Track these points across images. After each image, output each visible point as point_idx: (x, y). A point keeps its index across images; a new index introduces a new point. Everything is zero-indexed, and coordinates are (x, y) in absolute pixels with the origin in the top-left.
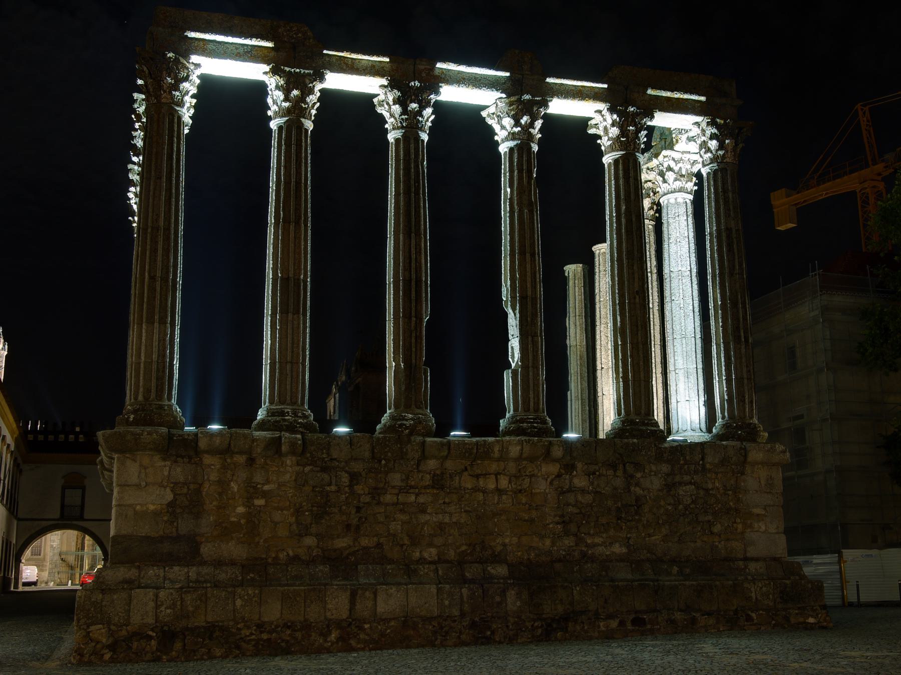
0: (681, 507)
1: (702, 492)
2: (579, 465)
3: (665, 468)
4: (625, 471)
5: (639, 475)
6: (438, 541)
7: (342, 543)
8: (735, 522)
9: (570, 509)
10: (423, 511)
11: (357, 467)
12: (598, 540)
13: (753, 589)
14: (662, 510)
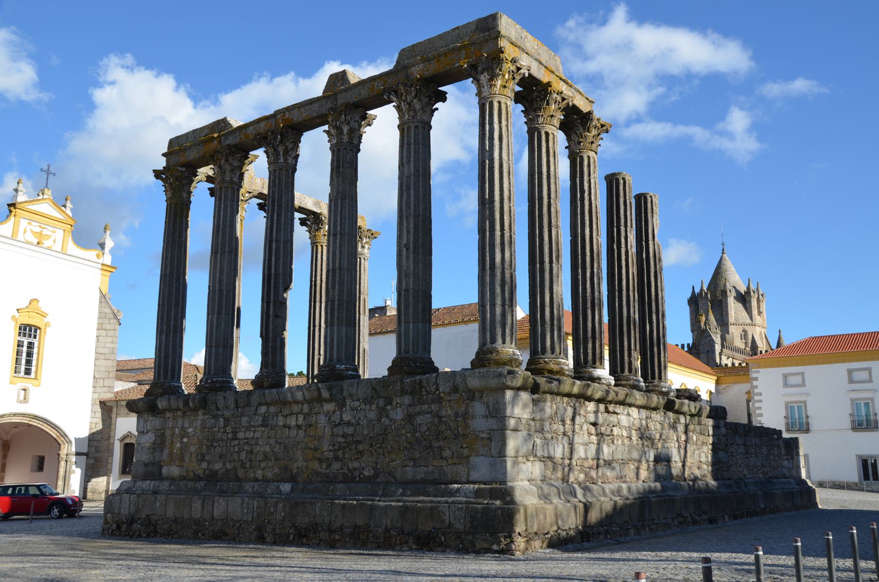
0: (418, 434)
1: (436, 420)
2: (348, 402)
3: (407, 400)
4: (377, 407)
5: (389, 407)
6: (263, 465)
7: (218, 466)
8: (462, 447)
9: (340, 439)
10: (257, 444)
11: (227, 414)
12: (356, 464)
13: (447, 513)
14: (403, 438)
